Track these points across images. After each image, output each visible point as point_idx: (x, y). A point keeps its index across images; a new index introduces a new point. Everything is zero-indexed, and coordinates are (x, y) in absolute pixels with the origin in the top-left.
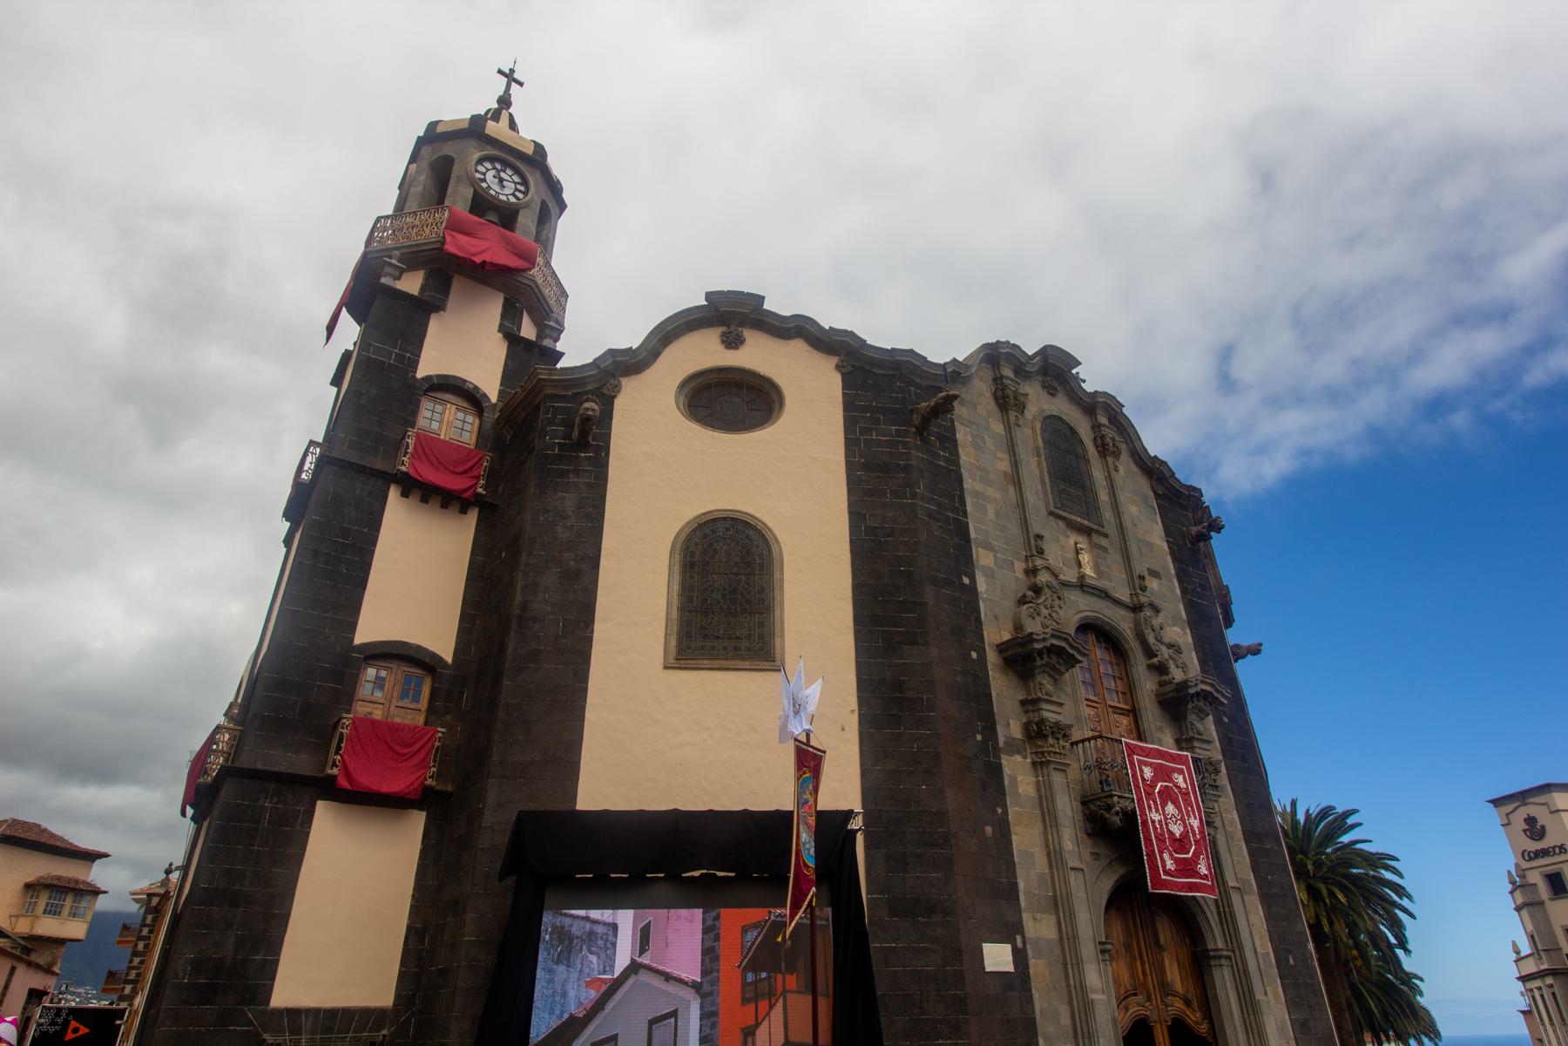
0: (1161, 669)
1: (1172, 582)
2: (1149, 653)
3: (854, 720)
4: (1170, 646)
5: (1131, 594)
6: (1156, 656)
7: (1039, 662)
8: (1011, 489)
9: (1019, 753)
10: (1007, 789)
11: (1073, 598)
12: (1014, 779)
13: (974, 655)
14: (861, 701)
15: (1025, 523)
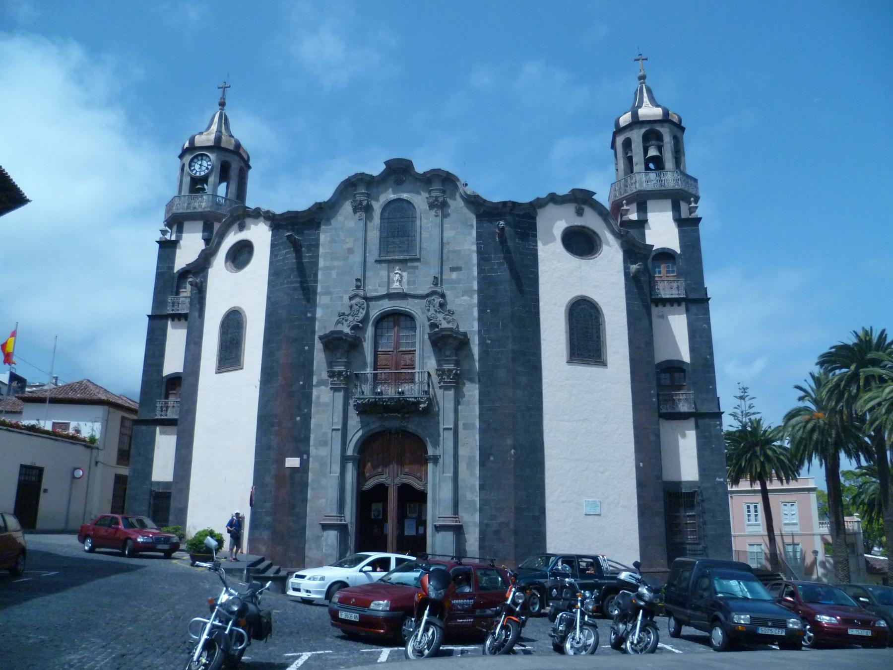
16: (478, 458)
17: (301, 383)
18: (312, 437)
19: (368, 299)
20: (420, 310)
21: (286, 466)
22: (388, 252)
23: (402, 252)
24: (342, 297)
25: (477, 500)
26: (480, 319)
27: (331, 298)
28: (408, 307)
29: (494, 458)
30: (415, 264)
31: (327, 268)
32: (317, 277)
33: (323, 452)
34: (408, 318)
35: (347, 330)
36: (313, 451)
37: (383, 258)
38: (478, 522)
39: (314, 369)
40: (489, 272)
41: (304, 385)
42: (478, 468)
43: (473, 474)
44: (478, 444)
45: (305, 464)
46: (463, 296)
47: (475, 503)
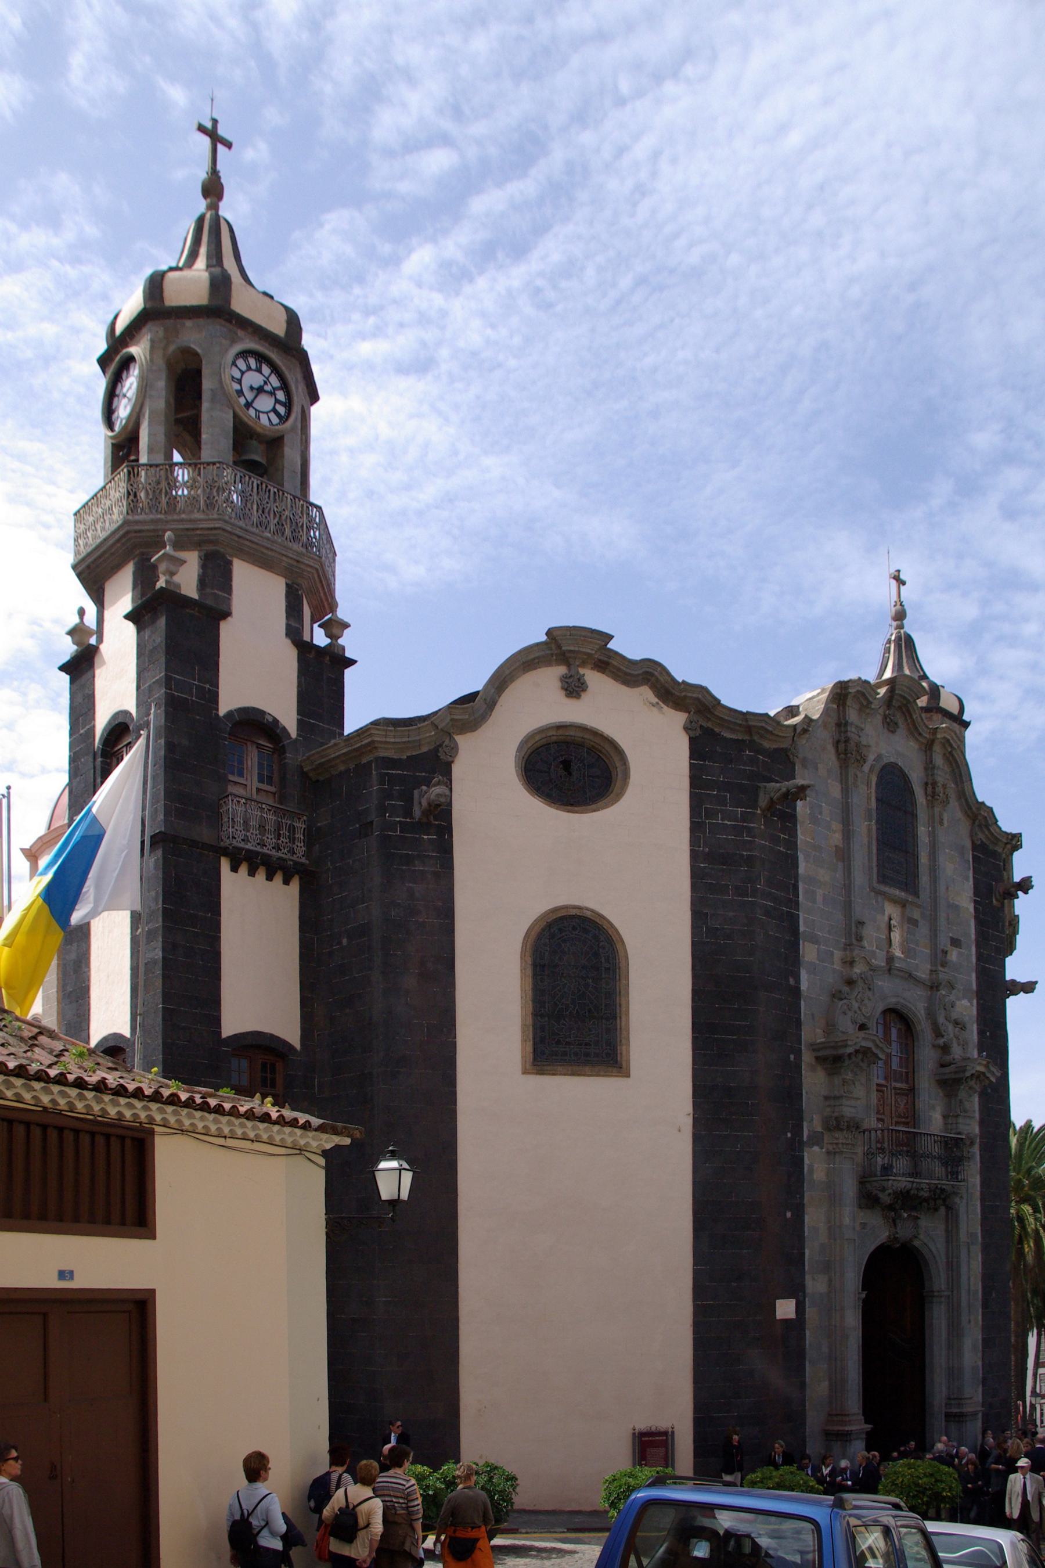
0: (945, 1049)
1: (970, 951)
2: (938, 1034)
3: (689, 1122)
4: (956, 1023)
5: (931, 971)
6: (943, 1036)
7: (847, 1063)
8: (840, 865)
11: (880, 983)
12: (811, 1167)
13: (792, 1057)
14: (696, 1105)
15: (848, 906)
21: (778, 1317)
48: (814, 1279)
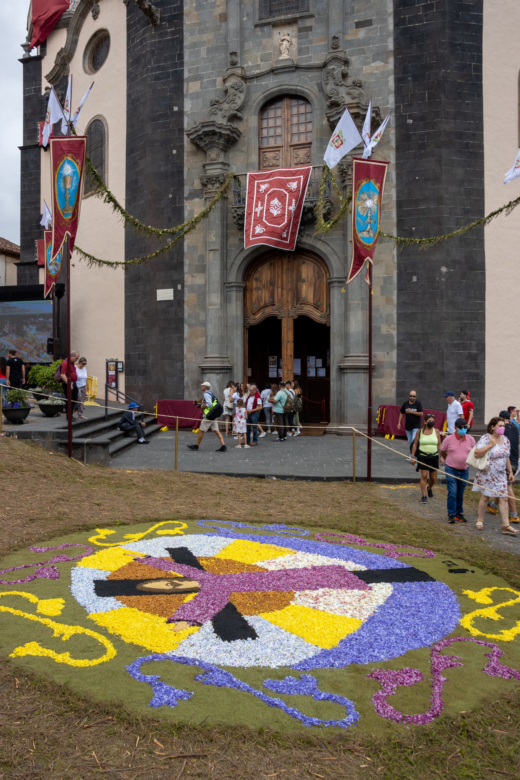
9: (197, 197)
10: (185, 217)
16: (395, 279)
17: (170, 196)
18: (187, 262)
19: (245, 79)
20: (316, 87)
21: (158, 300)
22: (271, 12)
23: (289, 10)
24: (215, 81)
25: (395, 333)
26: (398, 91)
27: (201, 83)
28: (299, 84)
29: (418, 279)
30: (309, 23)
31: (194, 45)
32: (183, 59)
33: (199, 280)
34: (301, 102)
35: (224, 122)
36: (188, 279)
37: (264, 21)
38: (396, 362)
39: (185, 177)
40: (410, 22)
41: (174, 198)
42: (395, 292)
43: (389, 301)
44: (395, 260)
45: (179, 296)
46: (373, 62)
47: (393, 338)
48: (193, 276)
